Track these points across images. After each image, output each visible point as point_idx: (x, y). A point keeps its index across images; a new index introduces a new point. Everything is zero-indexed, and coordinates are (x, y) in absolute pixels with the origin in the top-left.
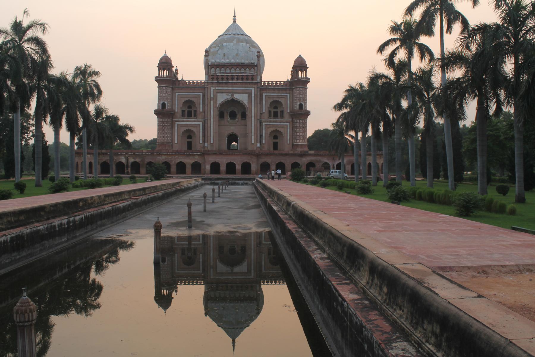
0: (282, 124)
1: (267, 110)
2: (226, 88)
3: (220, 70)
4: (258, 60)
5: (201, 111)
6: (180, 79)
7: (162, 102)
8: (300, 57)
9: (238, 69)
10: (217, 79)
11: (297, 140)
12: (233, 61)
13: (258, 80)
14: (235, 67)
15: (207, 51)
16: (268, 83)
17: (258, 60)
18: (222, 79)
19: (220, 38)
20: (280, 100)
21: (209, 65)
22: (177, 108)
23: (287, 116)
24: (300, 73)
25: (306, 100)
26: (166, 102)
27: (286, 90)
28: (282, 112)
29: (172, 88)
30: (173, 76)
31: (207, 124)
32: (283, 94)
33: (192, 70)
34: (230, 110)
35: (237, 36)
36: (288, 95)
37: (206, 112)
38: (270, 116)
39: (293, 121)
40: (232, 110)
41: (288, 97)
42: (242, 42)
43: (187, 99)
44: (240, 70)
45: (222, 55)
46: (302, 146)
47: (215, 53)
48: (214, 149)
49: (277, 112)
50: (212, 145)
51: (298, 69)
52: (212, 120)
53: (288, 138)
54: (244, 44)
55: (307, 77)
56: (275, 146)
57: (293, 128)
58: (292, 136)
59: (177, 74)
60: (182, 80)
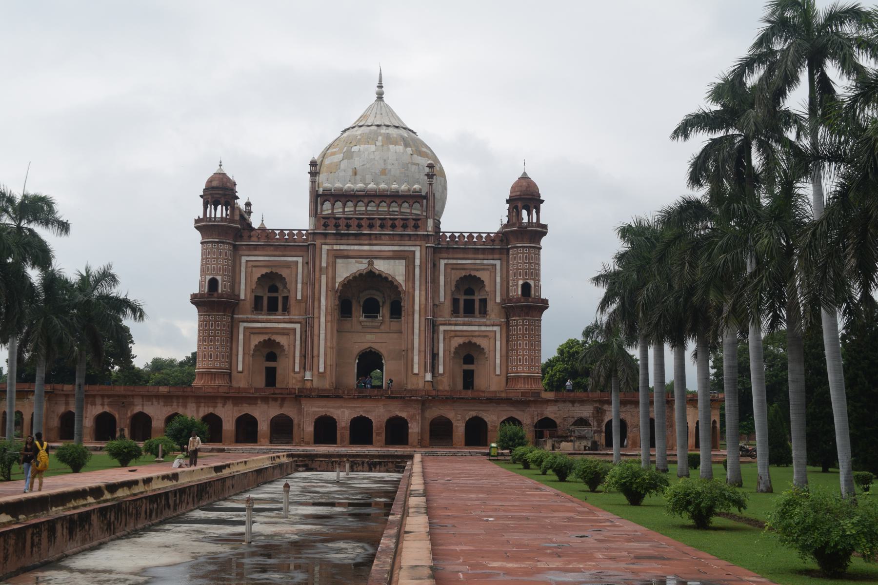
0: (483, 328)
1: (449, 297)
2: (356, 247)
3: (344, 206)
4: (431, 184)
5: (299, 297)
6: (256, 224)
7: (208, 277)
8: (525, 177)
9: (384, 204)
10: (337, 226)
11: (517, 366)
12: (372, 186)
13: (430, 229)
14: (377, 201)
15: (313, 164)
16: (453, 236)
17: (431, 184)
18: (348, 226)
19: (345, 135)
20: (478, 274)
21: (318, 196)
22: (244, 292)
24: (524, 213)
25: (538, 275)
26: (219, 278)
27: (492, 251)
28: (484, 302)
29: (235, 246)
30: (237, 217)
31: (313, 327)
32: (485, 262)
33: (281, 206)
34: (365, 296)
35: (384, 130)
36: (498, 263)
37: (310, 300)
38: (455, 312)
39: (507, 322)
40: (369, 297)
41: (498, 267)
42: (396, 143)
43: (268, 270)
44: (389, 206)
45: (350, 172)
48: (328, 387)
49: (474, 300)
50: (322, 375)
51: (520, 205)
52: (323, 319)
53: (498, 361)
54: (400, 148)
55: (541, 222)
58: (506, 357)
59: (249, 213)
60: (263, 229)
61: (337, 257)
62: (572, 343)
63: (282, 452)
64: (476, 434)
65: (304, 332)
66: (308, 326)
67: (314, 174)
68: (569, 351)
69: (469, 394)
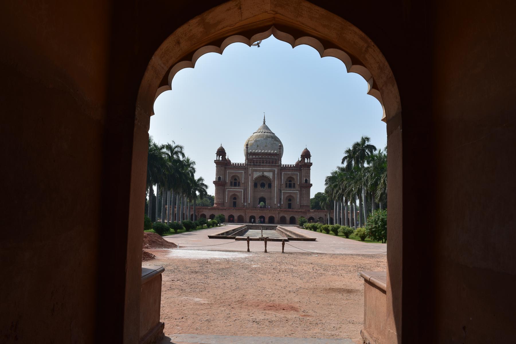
15: (247, 145)
18: (257, 163)
19: (255, 134)
23: (297, 186)
28: (294, 184)
29: (225, 168)
35: (266, 134)
37: (246, 182)
38: (286, 187)
40: (263, 183)
42: (269, 137)
45: (256, 146)
46: (308, 206)
47: (252, 145)
50: (249, 204)
56: (290, 206)
57: (301, 195)
61: (253, 171)
62: (319, 193)
63: (244, 225)
64: (292, 222)
65: (244, 192)
66: (245, 190)
67: (247, 148)
68: (318, 195)
69: (290, 210)
